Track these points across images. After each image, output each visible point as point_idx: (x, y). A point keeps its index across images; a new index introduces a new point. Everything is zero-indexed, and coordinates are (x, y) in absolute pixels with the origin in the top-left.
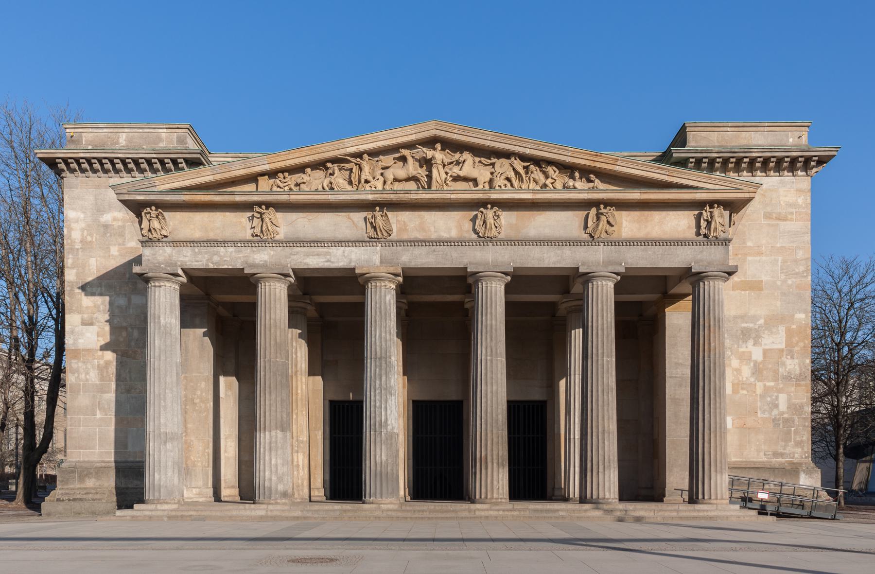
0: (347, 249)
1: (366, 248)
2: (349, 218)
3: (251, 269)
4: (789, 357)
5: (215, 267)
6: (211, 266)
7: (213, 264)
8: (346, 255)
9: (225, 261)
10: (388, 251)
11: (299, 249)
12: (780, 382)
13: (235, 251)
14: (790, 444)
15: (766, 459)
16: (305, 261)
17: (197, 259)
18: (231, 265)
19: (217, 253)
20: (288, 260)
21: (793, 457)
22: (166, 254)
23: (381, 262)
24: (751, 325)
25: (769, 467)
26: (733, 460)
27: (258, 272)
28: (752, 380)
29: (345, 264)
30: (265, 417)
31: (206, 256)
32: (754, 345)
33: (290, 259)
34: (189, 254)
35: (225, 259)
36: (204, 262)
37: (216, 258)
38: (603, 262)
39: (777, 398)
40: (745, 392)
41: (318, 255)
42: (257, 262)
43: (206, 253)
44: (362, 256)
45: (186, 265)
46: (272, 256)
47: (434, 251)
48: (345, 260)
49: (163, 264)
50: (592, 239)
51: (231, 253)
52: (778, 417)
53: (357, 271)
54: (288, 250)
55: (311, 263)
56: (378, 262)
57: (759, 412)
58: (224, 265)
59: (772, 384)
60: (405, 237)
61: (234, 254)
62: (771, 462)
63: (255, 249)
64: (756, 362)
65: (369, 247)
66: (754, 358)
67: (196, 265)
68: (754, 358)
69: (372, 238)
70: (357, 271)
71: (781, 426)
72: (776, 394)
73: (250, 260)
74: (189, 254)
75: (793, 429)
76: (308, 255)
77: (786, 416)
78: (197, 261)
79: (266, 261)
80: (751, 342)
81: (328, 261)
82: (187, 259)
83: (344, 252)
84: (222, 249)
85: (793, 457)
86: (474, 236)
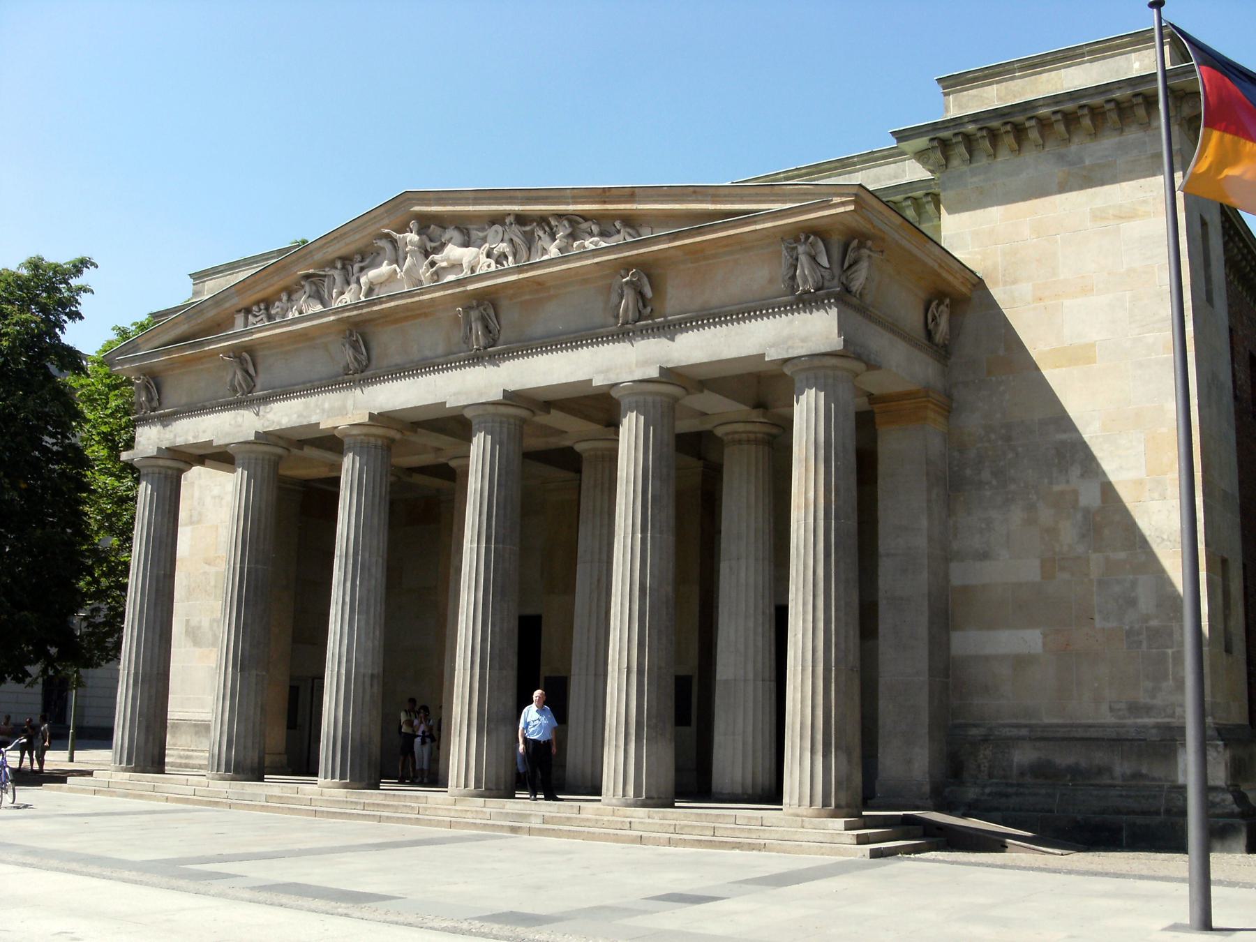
4: (1156, 495)
12: (1139, 551)
14: (1164, 685)
15: (1113, 720)
21: (1173, 716)
25: (1114, 736)
28: (1080, 549)
32: (1082, 475)
39: (1134, 584)
40: (1066, 576)
52: (1137, 626)
53: (322, 427)
57: (1097, 617)
59: (1122, 555)
62: (1123, 726)
64: (1087, 511)
66: (1083, 501)
68: (1083, 501)
70: (322, 427)
71: (1145, 645)
72: (1131, 577)
75: (1170, 651)
77: (1154, 623)
82: (172, 436)
85: (1173, 716)
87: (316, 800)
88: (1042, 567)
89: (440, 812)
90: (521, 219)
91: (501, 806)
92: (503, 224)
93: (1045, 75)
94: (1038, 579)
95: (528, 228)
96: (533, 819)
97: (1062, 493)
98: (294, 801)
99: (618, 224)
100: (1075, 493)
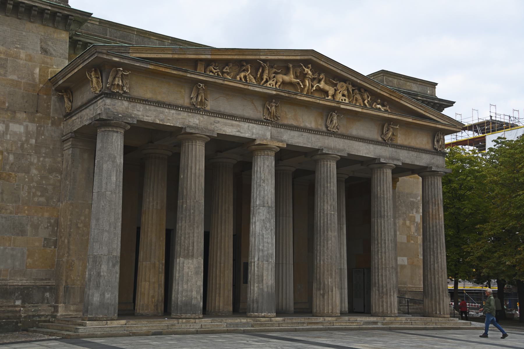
0: (251, 125)
1: (262, 126)
2: (253, 103)
3: (191, 130)
5: (161, 123)
6: (158, 122)
7: (159, 120)
8: (250, 129)
9: (168, 119)
10: (275, 130)
11: (220, 119)
13: (176, 113)
16: (224, 129)
17: (148, 115)
18: (173, 124)
19: (162, 113)
20: (212, 126)
22: (123, 106)
23: (271, 138)
24: (415, 200)
26: (408, 286)
27: (196, 132)
29: (250, 136)
30: (193, 246)
31: (154, 113)
32: (416, 212)
33: (214, 126)
34: (141, 109)
35: (169, 118)
36: (153, 118)
37: (162, 116)
38: (389, 157)
41: (232, 125)
42: (191, 124)
43: (155, 111)
44: (260, 132)
45: (139, 118)
46: (202, 121)
47: (302, 135)
48: (249, 132)
49: (120, 114)
50: (384, 142)
51: (173, 114)
54: (213, 119)
55: (228, 131)
56: (269, 137)
58: (167, 123)
60: (285, 122)
61: (175, 115)
63: (190, 114)
65: (264, 126)
67: (146, 119)
69: (267, 120)
73: (186, 123)
74: (141, 109)
76: (226, 124)
78: (147, 116)
79: (197, 124)
80: (415, 211)
81: (239, 131)
82: (140, 113)
83: (249, 127)
84: (167, 110)
86: (324, 129)
87: (282, 323)
88: (407, 238)
89: (342, 324)
90: (354, 84)
91: (356, 320)
92: (346, 83)
93: (408, 83)
94: (406, 242)
95: (354, 88)
96: (379, 324)
97: (411, 216)
98: (269, 325)
99: (386, 103)
100: (415, 217)
